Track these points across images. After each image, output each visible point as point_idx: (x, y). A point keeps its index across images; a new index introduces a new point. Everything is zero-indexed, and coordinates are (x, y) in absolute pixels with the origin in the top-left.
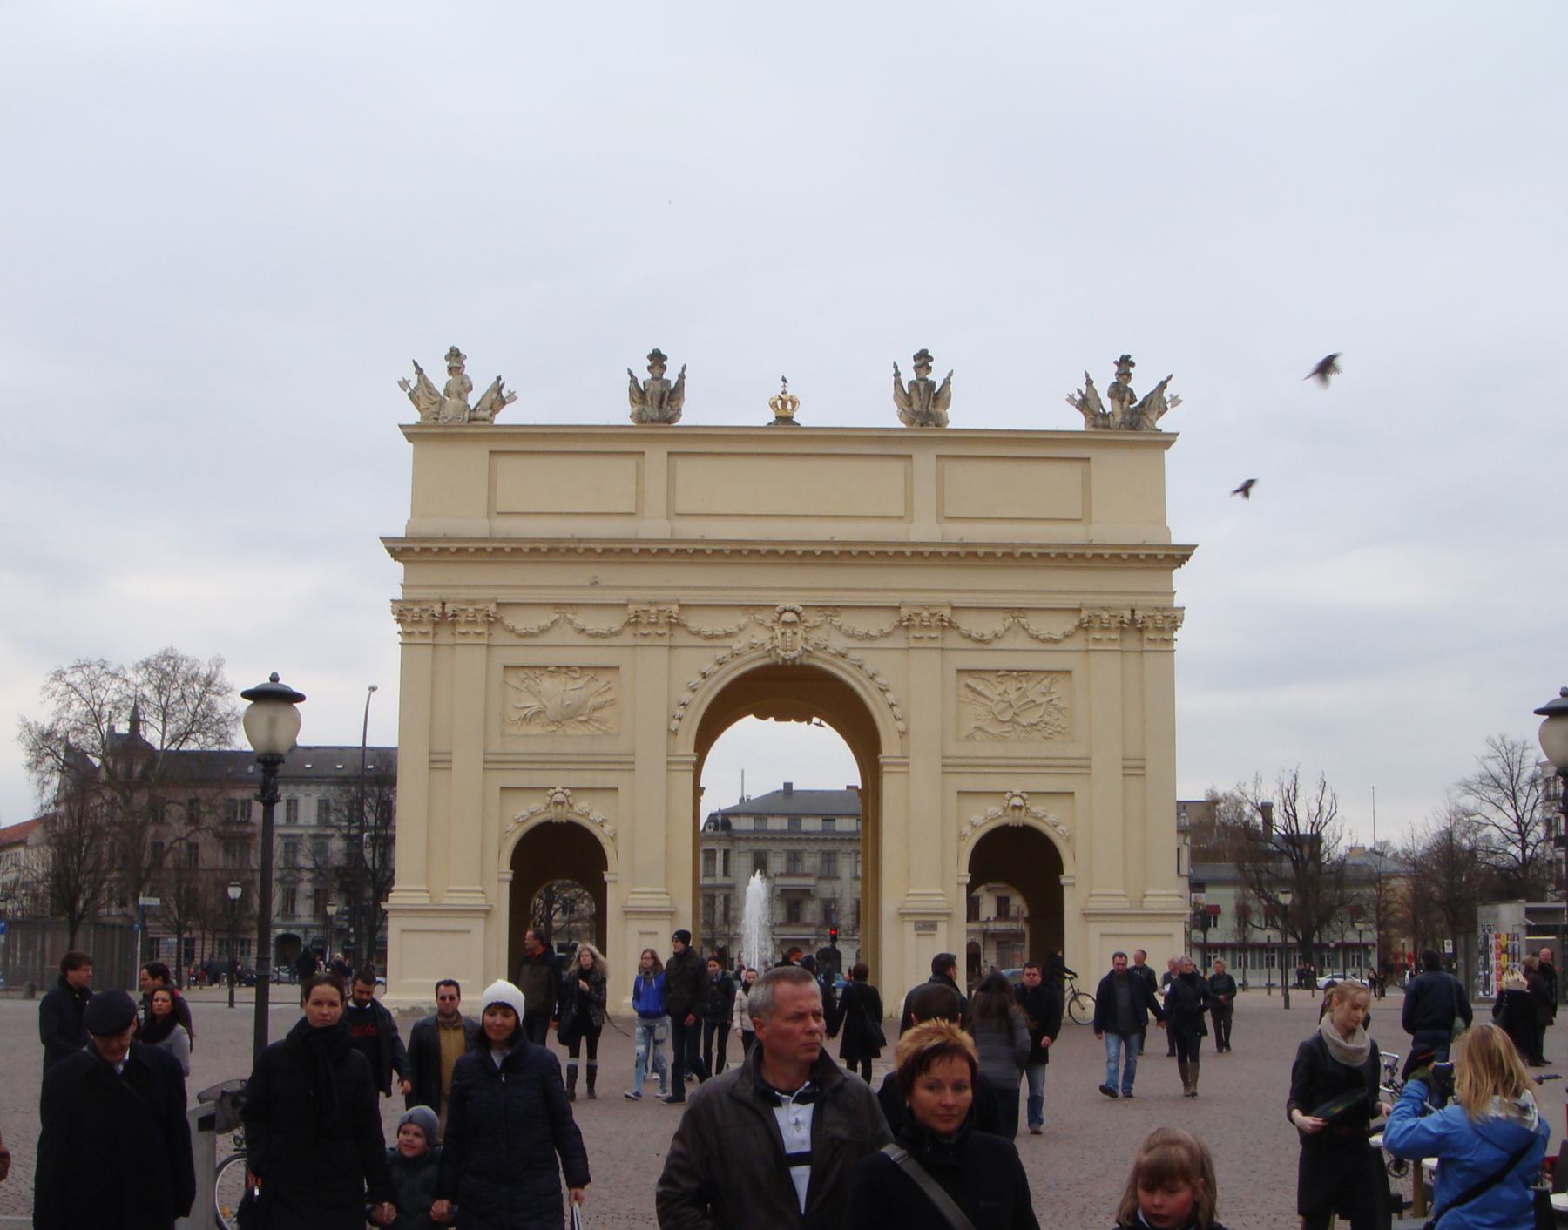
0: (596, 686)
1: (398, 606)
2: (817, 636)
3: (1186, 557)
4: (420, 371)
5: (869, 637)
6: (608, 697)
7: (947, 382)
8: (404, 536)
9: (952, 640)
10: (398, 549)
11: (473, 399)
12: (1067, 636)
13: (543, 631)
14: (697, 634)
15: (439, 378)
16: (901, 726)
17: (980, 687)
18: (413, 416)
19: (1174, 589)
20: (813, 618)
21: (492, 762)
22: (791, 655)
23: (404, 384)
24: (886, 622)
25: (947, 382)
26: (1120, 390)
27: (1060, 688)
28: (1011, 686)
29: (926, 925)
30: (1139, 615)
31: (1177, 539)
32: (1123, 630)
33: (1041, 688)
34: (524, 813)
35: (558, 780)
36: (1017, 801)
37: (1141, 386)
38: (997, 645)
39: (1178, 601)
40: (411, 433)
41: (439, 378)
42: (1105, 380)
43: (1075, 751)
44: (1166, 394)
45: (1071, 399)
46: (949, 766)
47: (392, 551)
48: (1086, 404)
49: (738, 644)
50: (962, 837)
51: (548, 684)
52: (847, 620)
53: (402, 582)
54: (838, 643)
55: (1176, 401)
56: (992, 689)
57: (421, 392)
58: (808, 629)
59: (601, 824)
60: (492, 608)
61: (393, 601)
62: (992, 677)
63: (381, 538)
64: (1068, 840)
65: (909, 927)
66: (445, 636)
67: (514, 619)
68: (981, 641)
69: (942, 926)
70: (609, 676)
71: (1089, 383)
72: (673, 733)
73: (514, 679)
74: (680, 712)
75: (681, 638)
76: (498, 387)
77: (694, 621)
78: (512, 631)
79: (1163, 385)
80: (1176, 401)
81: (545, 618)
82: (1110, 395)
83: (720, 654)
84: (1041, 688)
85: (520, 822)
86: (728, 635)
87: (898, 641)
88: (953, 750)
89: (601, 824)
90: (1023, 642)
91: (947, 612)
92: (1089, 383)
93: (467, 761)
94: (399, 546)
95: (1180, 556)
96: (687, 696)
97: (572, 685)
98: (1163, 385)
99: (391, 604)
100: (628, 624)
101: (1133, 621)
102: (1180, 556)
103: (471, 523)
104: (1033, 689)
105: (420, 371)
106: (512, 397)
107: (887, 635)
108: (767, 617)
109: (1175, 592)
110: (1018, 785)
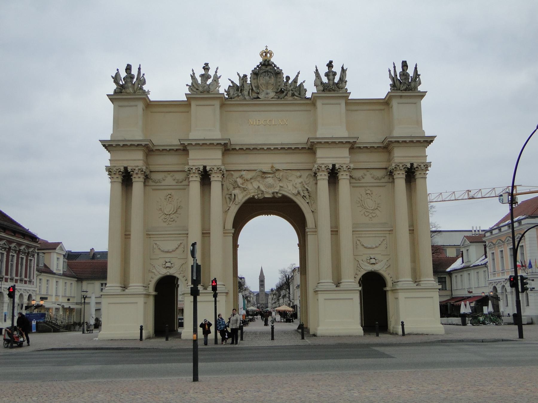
1: (107, 168)
3: (432, 141)
8: (110, 139)
10: (108, 146)
19: (427, 155)
31: (428, 133)
47: (104, 146)
53: (110, 159)
61: (105, 166)
63: (99, 140)
82: (400, 75)
94: (107, 144)
95: (429, 141)
99: (105, 167)
102: (429, 141)
109: (427, 156)
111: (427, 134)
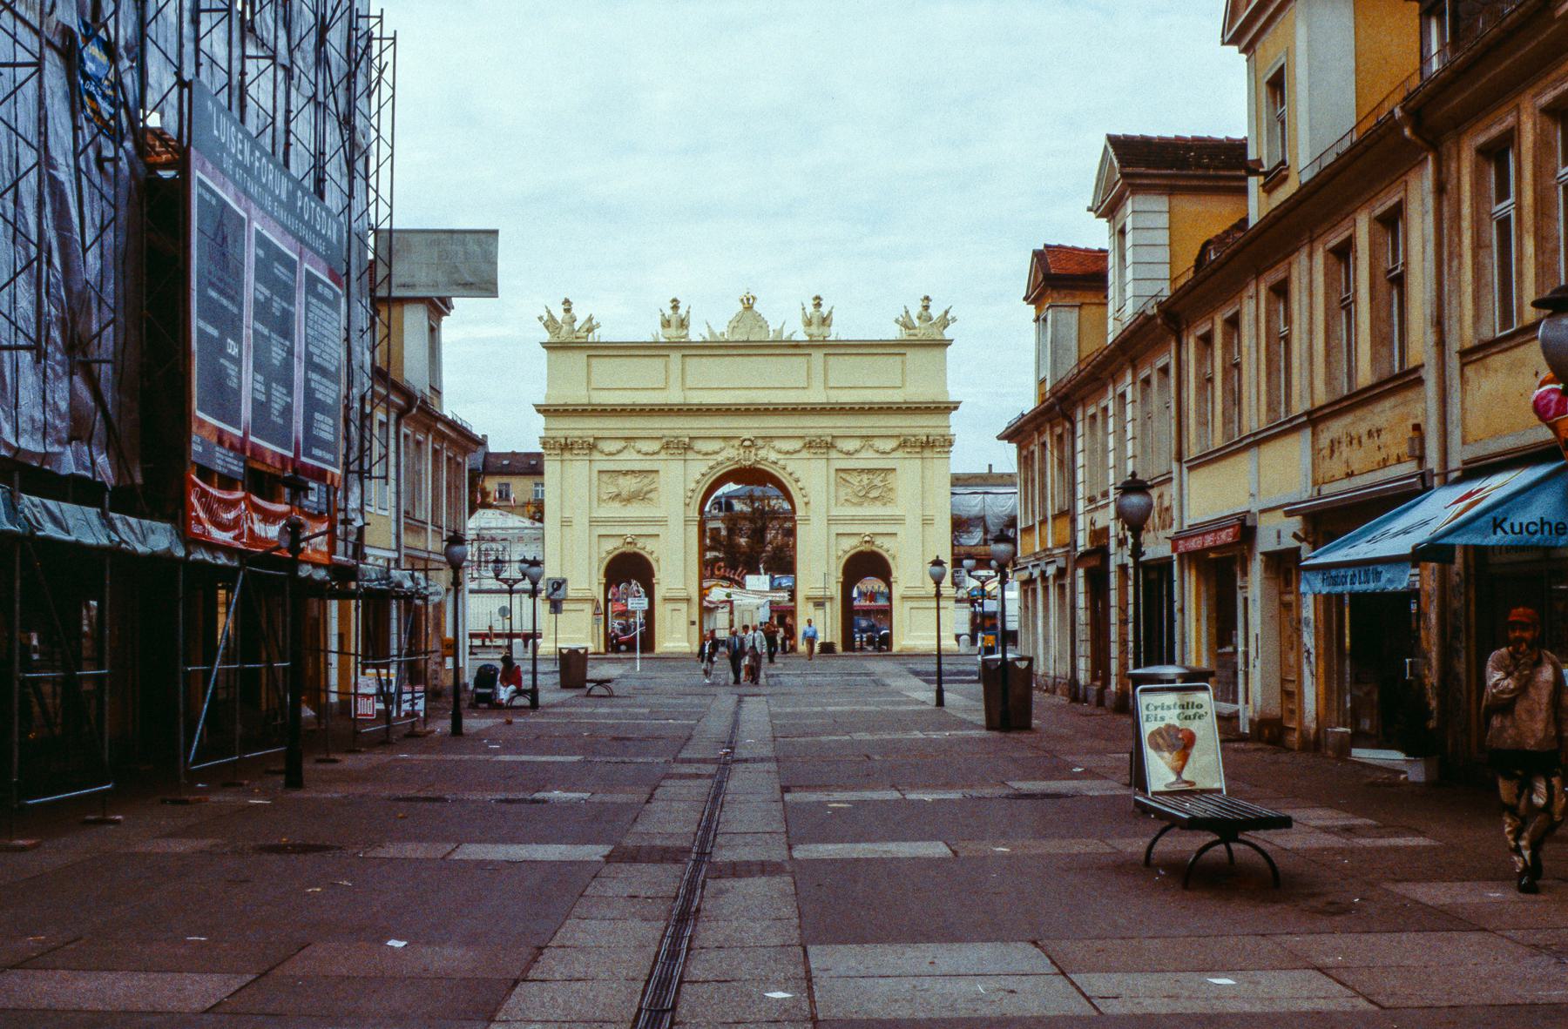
0: (646, 481)
2: (762, 453)
3: (956, 408)
4: (549, 312)
5: (788, 453)
6: (652, 487)
7: (830, 313)
9: (833, 454)
11: (577, 326)
12: (894, 450)
13: (619, 452)
14: (699, 452)
15: (559, 315)
16: (806, 500)
17: (848, 478)
18: (546, 336)
20: (760, 443)
21: (593, 522)
22: (748, 463)
23: (540, 318)
24: (798, 444)
25: (830, 313)
26: (925, 316)
27: (891, 477)
28: (865, 477)
29: (819, 603)
30: (931, 439)
32: (922, 447)
33: (880, 478)
34: (611, 548)
35: (629, 531)
36: (867, 539)
37: (936, 312)
38: (856, 456)
39: (952, 431)
40: (549, 347)
41: (559, 315)
42: (915, 310)
43: (897, 512)
44: (949, 317)
45: (897, 321)
46: (831, 521)
47: (539, 411)
48: (907, 325)
49: (720, 458)
50: (839, 558)
51: (622, 481)
52: (778, 444)
54: (773, 456)
55: (954, 320)
56: (854, 479)
57: (550, 323)
58: (758, 449)
59: (652, 553)
60: (591, 440)
62: (855, 474)
64: (894, 558)
65: (811, 605)
66: (567, 456)
67: (603, 445)
68: (848, 453)
69: (828, 605)
70: (653, 475)
71: (907, 312)
72: (687, 505)
73: (605, 477)
74: (690, 494)
75: (690, 455)
76: (590, 319)
77: (699, 445)
78: (602, 452)
79: (946, 312)
80: (954, 320)
81: (620, 445)
83: (711, 463)
84: (880, 478)
85: (608, 553)
86: (717, 453)
87: (804, 454)
88: (835, 512)
89: (652, 553)
90: (871, 454)
91: (829, 439)
92: (907, 312)
93: (581, 521)
95: (955, 406)
96: (693, 486)
97: (634, 481)
98: (946, 312)
100: (663, 448)
101: (928, 441)
102: (955, 406)
103: (577, 394)
104: (877, 481)
105: (549, 312)
106: (598, 325)
107: (799, 451)
108: (737, 443)
110: (868, 529)
111: (951, 399)
